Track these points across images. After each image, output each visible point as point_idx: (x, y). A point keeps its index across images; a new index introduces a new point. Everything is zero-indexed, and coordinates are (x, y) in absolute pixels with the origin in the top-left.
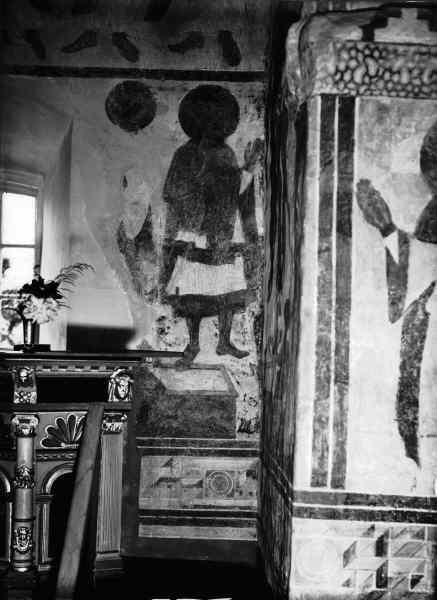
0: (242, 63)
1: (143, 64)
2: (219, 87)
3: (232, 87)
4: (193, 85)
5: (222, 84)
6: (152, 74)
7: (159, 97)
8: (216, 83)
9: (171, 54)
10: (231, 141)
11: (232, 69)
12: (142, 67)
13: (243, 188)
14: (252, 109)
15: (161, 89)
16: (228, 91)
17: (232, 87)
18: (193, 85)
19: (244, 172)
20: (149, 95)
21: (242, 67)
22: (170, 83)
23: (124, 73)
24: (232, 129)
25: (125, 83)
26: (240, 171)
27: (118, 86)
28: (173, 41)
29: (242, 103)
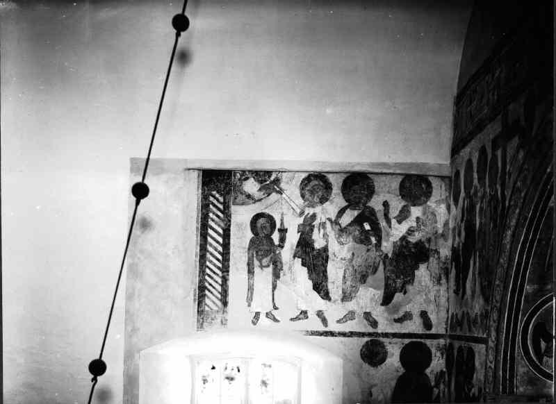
0: (433, 329)
1: (380, 329)
2: (421, 343)
3: (428, 342)
4: (407, 341)
5: (422, 340)
6: (386, 335)
7: (389, 348)
8: (419, 340)
9: (394, 323)
10: (428, 371)
11: (428, 332)
12: (380, 332)
13: (434, 397)
14: (438, 354)
15: (390, 343)
16: (425, 345)
17: (428, 342)
18: (407, 341)
19: (435, 389)
20: (383, 347)
21: (433, 331)
22: (395, 340)
23: (370, 335)
24: (428, 365)
25: (371, 341)
26: (432, 388)
27: (367, 342)
28: (396, 317)
29: (433, 350)
